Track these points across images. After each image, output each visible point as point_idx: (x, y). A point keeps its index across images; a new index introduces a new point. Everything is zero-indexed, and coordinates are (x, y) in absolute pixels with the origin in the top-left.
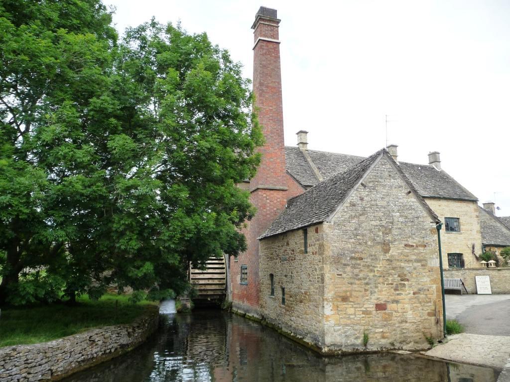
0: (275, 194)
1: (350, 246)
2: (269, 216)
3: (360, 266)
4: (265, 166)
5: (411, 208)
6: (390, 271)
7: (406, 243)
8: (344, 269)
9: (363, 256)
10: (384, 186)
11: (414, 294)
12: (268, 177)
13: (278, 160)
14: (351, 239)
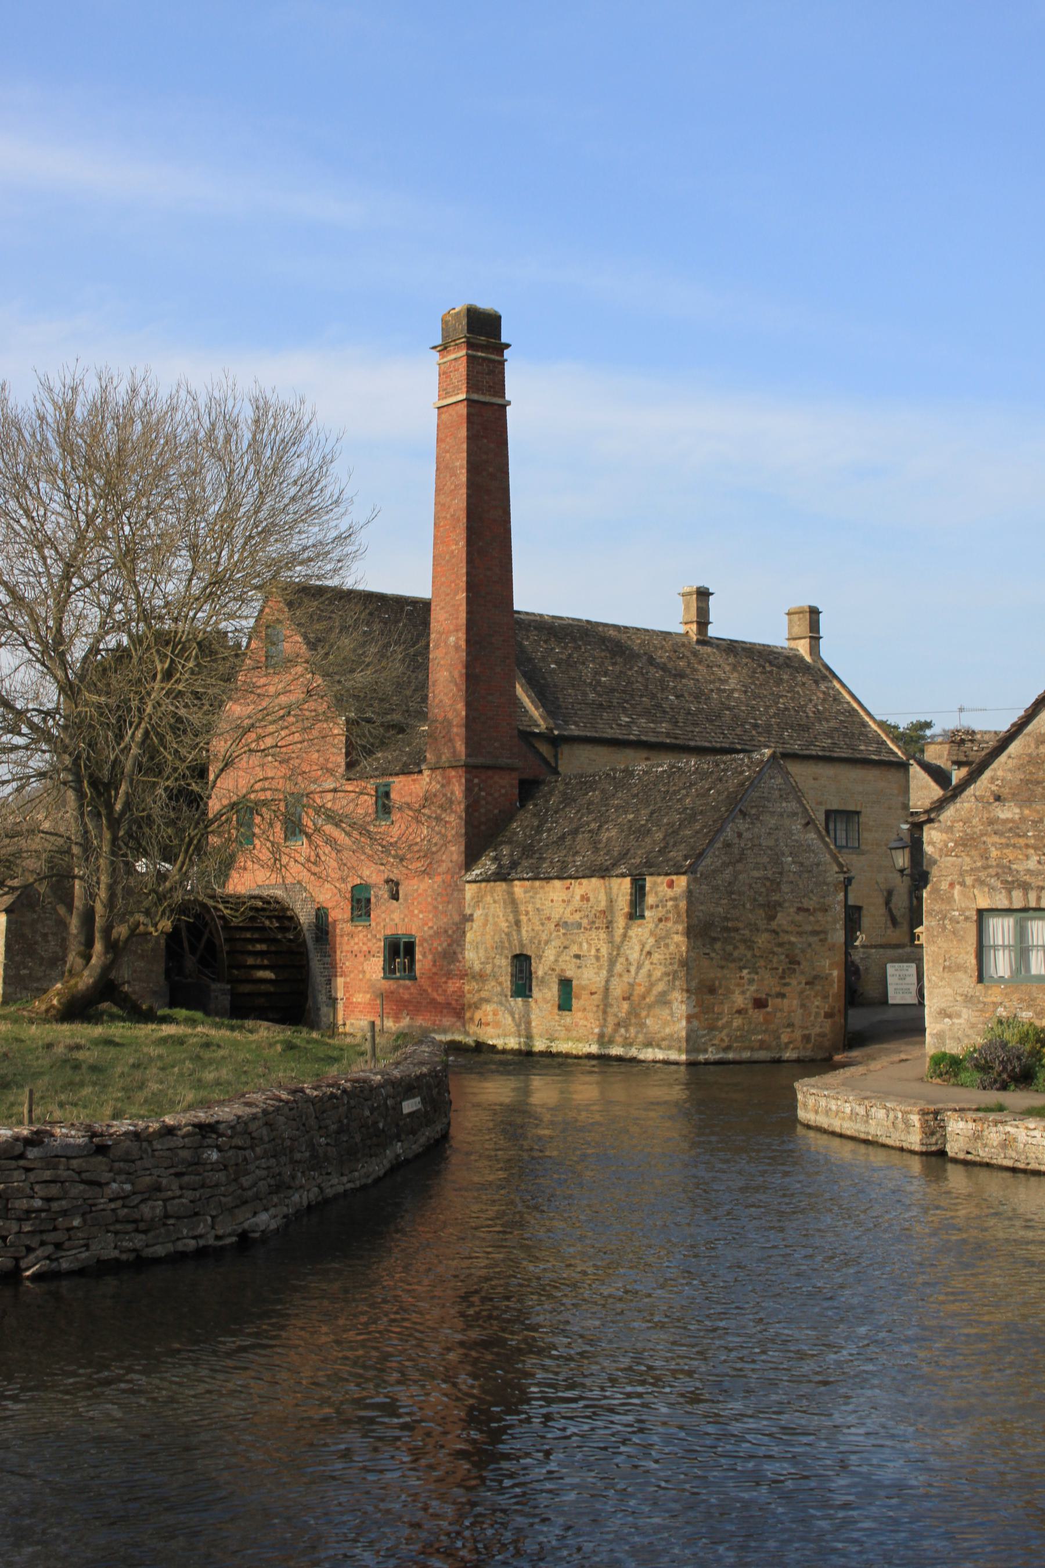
1: (721, 910)
2: (483, 828)
5: (809, 849)
6: (775, 949)
7: (800, 905)
9: (740, 925)
10: (773, 813)
11: (807, 983)
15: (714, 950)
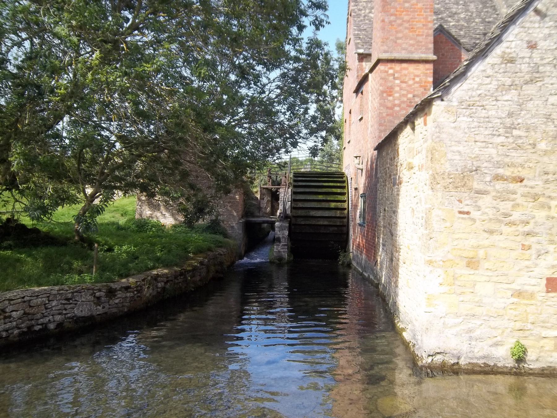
0: (411, 67)
1: (493, 151)
2: (397, 109)
3: (514, 196)
4: (392, 18)
8: (476, 202)
9: (523, 173)
12: (398, 38)
13: (420, 5)
14: (499, 135)
15: (479, 209)
